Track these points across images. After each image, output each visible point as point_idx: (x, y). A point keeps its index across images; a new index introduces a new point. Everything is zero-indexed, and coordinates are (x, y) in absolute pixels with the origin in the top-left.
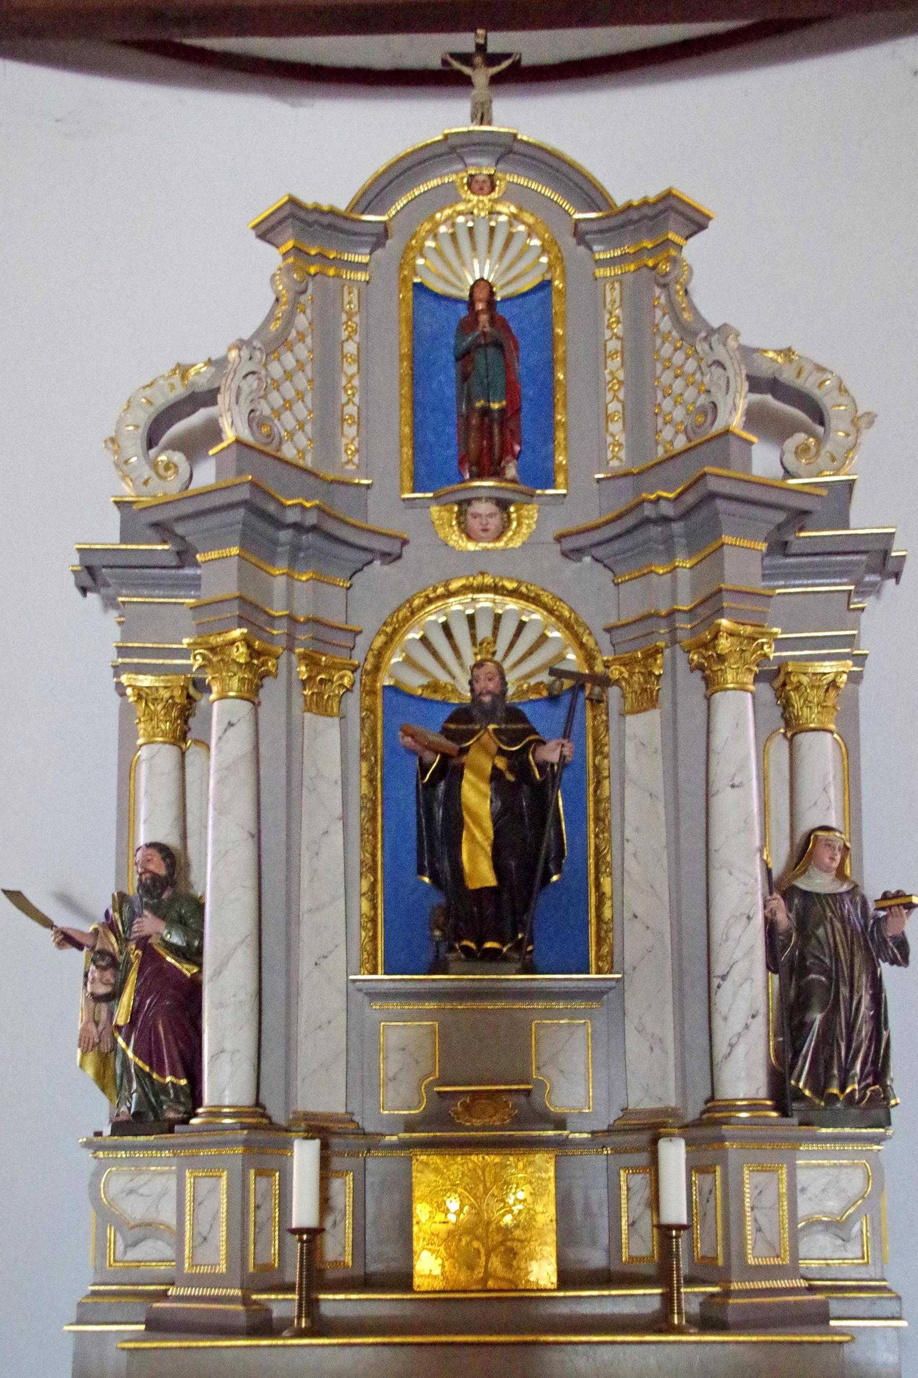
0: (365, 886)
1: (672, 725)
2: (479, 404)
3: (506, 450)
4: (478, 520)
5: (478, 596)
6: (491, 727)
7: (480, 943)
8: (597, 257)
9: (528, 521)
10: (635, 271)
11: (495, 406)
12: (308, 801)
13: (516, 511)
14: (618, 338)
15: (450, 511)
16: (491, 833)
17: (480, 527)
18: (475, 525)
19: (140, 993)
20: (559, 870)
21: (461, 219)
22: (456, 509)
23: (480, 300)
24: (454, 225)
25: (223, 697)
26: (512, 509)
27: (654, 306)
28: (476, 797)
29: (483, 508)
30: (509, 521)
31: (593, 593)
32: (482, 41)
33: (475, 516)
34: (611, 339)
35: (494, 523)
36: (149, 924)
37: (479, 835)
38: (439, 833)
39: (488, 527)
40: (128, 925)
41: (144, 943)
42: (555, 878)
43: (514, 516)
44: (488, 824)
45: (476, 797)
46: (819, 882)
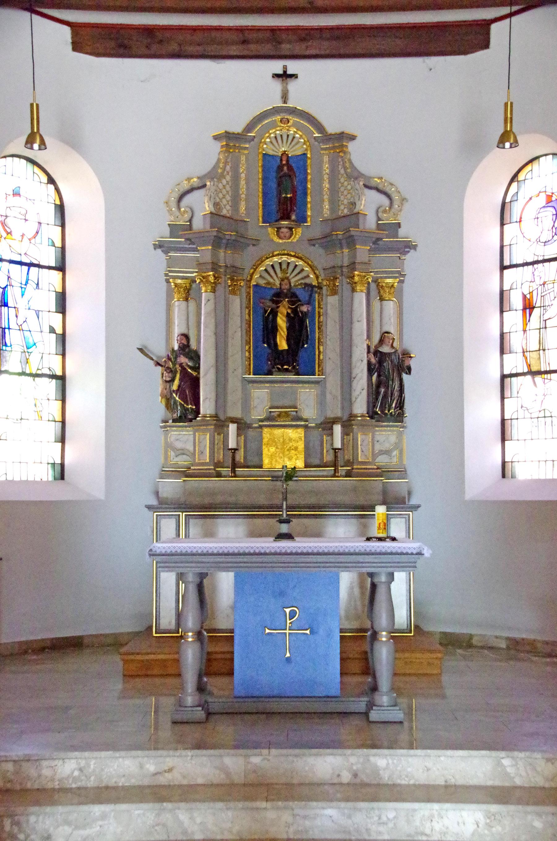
0: (247, 347)
1: (341, 302)
2: (283, 196)
3: (292, 210)
5: (283, 255)
6: (286, 300)
7: (282, 366)
11: (289, 196)
12: (231, 322)
16: (286, 333)
18: (282, 235)
19: (180, 380)
20: (307, 343)
21: (278, 132)
24: (276, 134)
25: (206, 292)
28: (282, 322)
29: (284, 230)
30: (292, 233)
31: (321, 258)
33: (282, 232)
35: (288, 235)
36: (183, 359)
37: (282, 334)
38: (270, 331)
40: (176, 358)
41: (181, 365)
42: (306, 346)
44: (285, 330)
45: (282, 322)
46: (385, 349)
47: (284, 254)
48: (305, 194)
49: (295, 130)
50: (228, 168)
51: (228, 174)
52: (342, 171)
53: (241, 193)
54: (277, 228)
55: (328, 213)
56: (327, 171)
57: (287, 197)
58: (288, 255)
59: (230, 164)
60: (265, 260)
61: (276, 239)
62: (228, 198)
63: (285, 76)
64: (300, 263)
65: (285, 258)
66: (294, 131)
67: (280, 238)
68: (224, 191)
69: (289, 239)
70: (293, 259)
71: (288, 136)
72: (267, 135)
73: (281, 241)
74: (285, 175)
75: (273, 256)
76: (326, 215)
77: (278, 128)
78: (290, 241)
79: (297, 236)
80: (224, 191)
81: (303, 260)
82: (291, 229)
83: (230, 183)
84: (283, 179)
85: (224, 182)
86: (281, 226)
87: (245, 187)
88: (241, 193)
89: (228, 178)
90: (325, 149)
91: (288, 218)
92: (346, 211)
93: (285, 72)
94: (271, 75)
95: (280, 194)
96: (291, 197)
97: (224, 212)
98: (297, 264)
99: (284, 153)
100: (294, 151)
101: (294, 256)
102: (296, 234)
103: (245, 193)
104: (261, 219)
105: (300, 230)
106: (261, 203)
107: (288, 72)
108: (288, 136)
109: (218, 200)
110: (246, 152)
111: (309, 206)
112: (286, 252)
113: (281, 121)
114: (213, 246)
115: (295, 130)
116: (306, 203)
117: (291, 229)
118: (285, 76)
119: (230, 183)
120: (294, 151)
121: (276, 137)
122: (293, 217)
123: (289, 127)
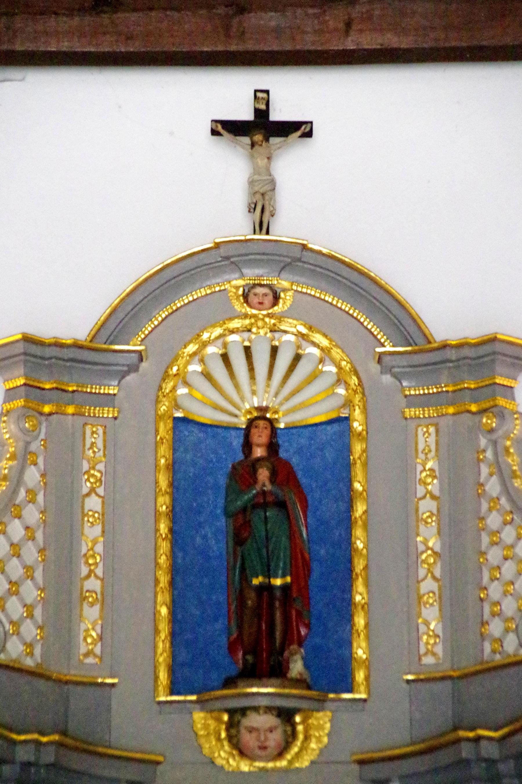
4: (254, 735)
15: (219, 720)
17: (257, 744)
22: (226, 717)
35: (275, 739)
69: (280, 755)
73: (245, 767)
79: (313, 745)
82: (286, 715)
102: (307, 738)
105: (323, 721)
117: (286, 715)
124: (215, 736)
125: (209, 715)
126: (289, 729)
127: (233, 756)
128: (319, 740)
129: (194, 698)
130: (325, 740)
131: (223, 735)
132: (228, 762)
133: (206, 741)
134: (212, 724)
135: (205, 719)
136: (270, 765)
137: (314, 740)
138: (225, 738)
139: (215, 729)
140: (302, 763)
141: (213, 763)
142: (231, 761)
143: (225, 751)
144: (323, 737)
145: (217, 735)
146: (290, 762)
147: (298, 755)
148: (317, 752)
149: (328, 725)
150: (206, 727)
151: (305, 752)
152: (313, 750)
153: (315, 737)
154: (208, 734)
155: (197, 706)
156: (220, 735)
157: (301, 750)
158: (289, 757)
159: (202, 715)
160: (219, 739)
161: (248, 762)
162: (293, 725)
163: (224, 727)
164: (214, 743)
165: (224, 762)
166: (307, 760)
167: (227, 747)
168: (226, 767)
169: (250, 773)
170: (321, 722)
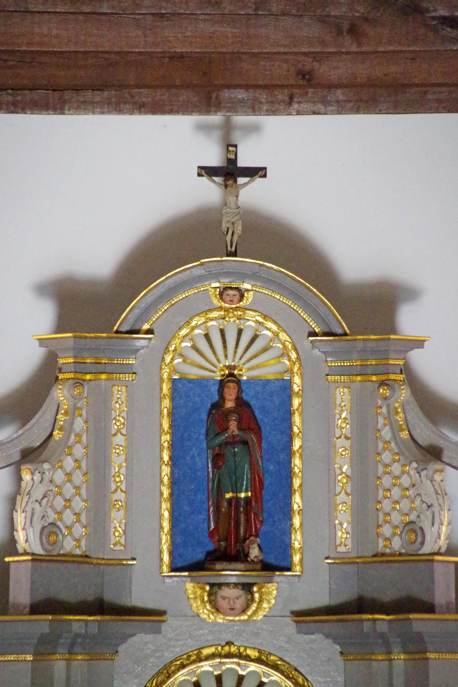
4: (227, 600)
8: (330, 364)
9: (272, 594)
10: (360, 381)
11: (243, 495)
13: (259, 591)
14: (347, 438)
15: (203, 589)
17: (228, 607)
18: (223, 604)
22: (208, 588)
23: (229, 400)
24: (207, 328)
26: (255, 589)
27: (377, 414)
30: (253, 600)
32: (233, 157)
33: (224, 598)
34: (340, 437)
35: (240, 603)
39: (235, 607)
43: (257, 596)
47: (229, 655)
48: (289, 493)
49: (261, 320)
50: (79, 424)
51: (79, 442)
52: (386, 433)
53: (113, 487)
54: (212, 585)
55: (349, 542)
56: (347, 430)
57: (238, 499)
58: (240, 656)
59: (84, 412)
60: (174, 672)
61: (205, 612)
62: (79, 504)
63: (229, 172)
64: (273, 678)
65: (230, 664)
66: (257, 322)
67: (217, 609)
68: (69, 491)
69: (244, 611)
70: (253, 667)
71: (240, 332)
72: (184, 332)
73: (220, 619)
74: (232, 442)
75: (199, 660)
76: (341, 549)
77: (215, 314)
78: (245, 617)
79: (265, 605)
80: (69, 491)
81: (282, 673)
82: (247, 587)
83: (83, 464)
84: (228, 451)
85: (69, 463)
86: (222, 580)
87: (123, 470)
88: (113, 487)
89: (79, 451)
90: (341, 372)
91: (237, 556)
92: (397, 544)
93: (232, 162)
94: (196, 171)
95: (220, 493)
96: (247, 500)
97: (69, 545)
98: (264, 680)
99: (231, 377)
100: (257, 367)
101: (259, 661)
102: (261, 601)
103: (123, 487)
104: (166, 558)
105: (272, 589)
106: (166, 514)
107: (242, 163)
108: (240, 332)
109: (52, 517)
110: (129, 377)
111: (297, 521)
112: (233, 649)
113: (221, 294)
114: (34, 655)
115: (261, 320)
116: (288, 513)
117: (247, 587)
118: (229, 172)
119: (83, 464)
120: (257, 367)
121: (207, 336)
122: (254, 552)
123: (245, 309)
124: (200, 600)
125: (196, 585)
126: (249, 597)
127: (213, 613)
128: (269, 602)
129: (186, 574)
130: (273, 601)
131: (206, 598)
132: (209, 616)
133: (194, 602)
134: (199, 592)
135: (194, 587)
136: (237, 618)
137: (265, 602)
138: (207, 601)
139: (200, 594)
140: (257, 617)
141: (199, 616)
142: (211, 616)
143: (207, 610)
144: (272, 599)
145: (202, 599)
146: (250, 617)
147: (255, 612)
148: (268, 610)
149: (275, 592)
150: (195, 593)
151: (260, 610)
152: (266, 608)
153: (266, 599)
154: (196, 597)
155: (189, 579)
156: (203, 599)
157: (257, 609)
158: (249, 613)
159: (192, 585)
160: (203, 601)
161: (222, 616)
162: (252, 594)
163: (206, 594)
164: (200, 604)
165: (206, 616)
166: (261, 615)
167: (208, 607)
168: (207, 619)
169: (223, 624)
170: (271, 590)
